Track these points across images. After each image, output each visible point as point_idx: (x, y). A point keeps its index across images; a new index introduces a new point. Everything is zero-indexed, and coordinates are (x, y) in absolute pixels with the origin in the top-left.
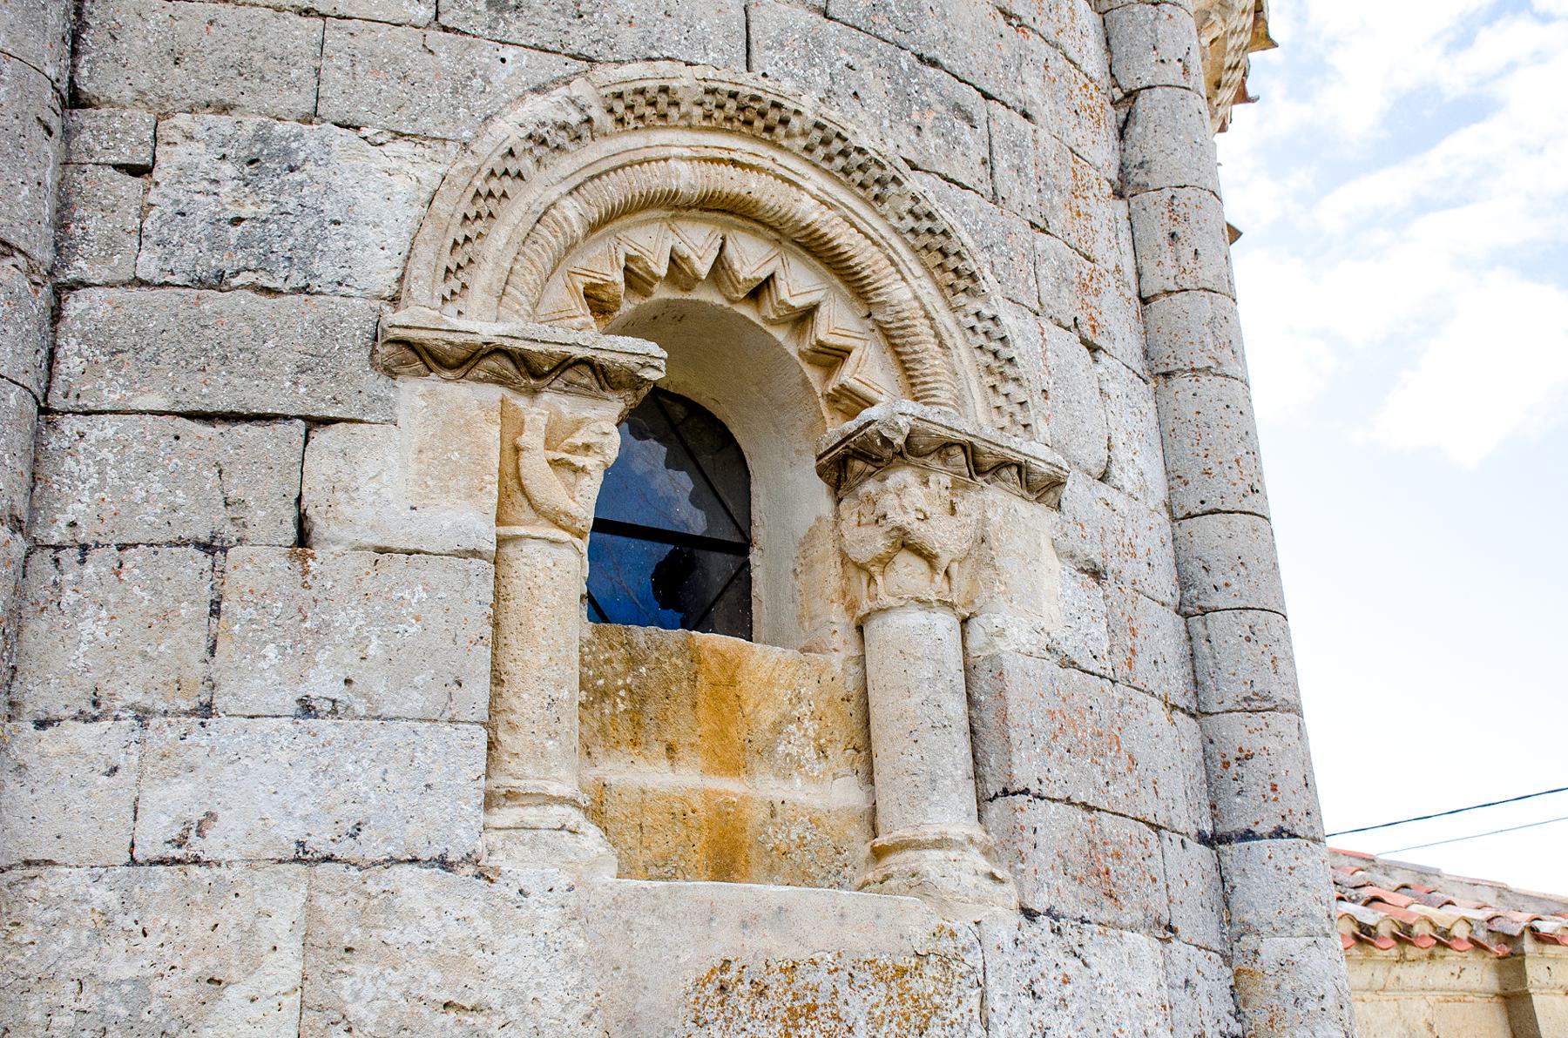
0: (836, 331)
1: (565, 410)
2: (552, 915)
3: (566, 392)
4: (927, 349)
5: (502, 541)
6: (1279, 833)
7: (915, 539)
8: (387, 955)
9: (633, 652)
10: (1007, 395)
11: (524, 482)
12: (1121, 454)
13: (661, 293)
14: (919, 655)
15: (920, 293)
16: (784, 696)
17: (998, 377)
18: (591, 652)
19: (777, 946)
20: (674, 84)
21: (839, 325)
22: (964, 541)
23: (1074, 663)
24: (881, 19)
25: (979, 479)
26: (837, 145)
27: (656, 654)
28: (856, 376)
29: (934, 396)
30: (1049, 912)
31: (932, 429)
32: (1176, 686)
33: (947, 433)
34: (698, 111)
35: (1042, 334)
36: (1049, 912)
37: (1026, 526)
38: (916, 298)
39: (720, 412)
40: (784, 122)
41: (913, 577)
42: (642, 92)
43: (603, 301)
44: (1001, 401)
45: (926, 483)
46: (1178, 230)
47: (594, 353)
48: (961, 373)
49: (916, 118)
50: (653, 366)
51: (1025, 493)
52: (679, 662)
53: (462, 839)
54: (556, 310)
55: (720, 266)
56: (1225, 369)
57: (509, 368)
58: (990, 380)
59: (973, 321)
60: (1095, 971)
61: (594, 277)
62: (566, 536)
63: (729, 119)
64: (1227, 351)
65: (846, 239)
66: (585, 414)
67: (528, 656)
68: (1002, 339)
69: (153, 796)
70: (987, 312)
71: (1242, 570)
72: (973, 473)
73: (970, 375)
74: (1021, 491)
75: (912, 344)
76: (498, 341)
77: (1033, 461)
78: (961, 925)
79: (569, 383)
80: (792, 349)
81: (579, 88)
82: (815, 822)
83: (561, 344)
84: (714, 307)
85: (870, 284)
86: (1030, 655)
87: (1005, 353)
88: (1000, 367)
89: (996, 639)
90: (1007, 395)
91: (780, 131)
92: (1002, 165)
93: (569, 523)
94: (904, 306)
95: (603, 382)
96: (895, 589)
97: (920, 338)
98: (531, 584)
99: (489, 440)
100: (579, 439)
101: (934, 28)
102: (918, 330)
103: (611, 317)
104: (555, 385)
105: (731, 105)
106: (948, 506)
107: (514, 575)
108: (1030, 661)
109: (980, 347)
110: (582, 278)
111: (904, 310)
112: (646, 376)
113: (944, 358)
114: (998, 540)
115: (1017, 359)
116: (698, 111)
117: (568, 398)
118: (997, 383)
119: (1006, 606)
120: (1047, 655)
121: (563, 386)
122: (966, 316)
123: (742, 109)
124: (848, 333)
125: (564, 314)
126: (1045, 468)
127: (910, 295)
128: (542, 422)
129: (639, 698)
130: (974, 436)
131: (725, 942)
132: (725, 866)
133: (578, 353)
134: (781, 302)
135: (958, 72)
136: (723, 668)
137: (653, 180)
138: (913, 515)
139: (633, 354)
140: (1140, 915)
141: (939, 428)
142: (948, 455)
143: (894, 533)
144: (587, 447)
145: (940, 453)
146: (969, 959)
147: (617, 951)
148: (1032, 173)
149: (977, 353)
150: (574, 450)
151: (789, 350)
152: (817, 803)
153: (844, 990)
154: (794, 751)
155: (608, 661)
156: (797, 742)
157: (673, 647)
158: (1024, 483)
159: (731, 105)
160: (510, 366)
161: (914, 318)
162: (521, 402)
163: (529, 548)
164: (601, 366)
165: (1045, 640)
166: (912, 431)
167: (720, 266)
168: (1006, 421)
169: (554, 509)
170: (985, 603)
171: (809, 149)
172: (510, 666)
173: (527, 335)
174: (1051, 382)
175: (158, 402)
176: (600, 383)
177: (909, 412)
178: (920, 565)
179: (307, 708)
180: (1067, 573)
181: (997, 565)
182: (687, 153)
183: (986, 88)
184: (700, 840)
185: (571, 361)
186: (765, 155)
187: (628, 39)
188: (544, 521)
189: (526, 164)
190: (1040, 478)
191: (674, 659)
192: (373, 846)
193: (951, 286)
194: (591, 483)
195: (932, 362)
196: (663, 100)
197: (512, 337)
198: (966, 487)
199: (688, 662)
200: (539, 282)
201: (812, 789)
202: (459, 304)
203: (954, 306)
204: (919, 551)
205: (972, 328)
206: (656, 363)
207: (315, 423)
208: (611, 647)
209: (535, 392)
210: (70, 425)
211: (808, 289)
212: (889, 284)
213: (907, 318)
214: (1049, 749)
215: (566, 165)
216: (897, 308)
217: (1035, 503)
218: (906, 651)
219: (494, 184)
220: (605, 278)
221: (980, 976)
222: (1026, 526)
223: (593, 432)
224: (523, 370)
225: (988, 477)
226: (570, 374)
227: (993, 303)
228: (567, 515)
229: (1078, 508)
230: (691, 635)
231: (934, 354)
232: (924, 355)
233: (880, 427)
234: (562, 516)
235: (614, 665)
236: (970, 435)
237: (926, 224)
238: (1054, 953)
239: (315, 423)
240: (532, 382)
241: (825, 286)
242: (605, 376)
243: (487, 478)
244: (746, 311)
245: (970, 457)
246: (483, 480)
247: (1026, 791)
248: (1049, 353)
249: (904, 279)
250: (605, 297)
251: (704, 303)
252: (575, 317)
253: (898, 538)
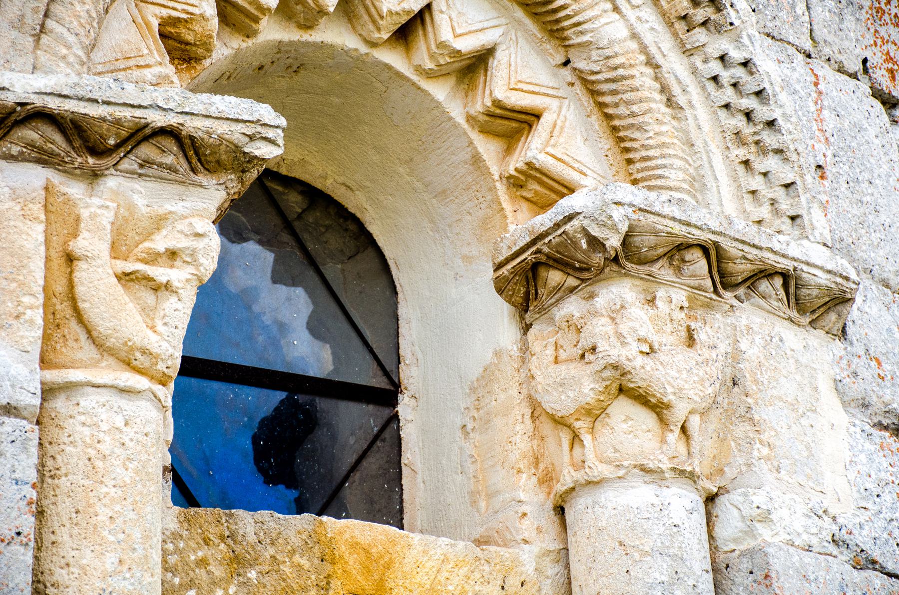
0: (520, 86)
1: (140, 201)
3: (140, 175)
4: (650, 111)
5: (48, 392)
7: (637, 381)
9: (238, 549)
10: (765, 174)
11: (82, 305)
14: (647, 548)
15: (640, 28)
17: (753, 148)
18: (177, 551)
21: (524, 77)
22: (707, 384)
23: (874, 562)
25: (728, 295)
27: (272, 551)
28: (549, 149)
29: (661, 177)
31: (662, 224)
33: (678, 229)
35: (816, 84)
37: (797, 361)
38: (634, 36)
39: (353, 202)
41: (636, 436)
43: (187, 43)
44: (757, 183)
45: (652, 301)
47: (180, 119)
48: (699, 143)
50: (265, 139)
51: (794, 314)
52: (304, 562)
54: (119, 55)
57: (57, 141)
58: (742, 153)
59: (715, 67)
61: (174, 9)
66: (168, 207)
67: (87, 558)
68: (759, 93)
70: (737, 55)
72: (719, 286)
73: (713, 147)
74: (788, 312)
75: (628, 103)
76: (39, 102)
77: (805, 268)
79: (146, 163)
80: (457, 111)
83: (133, 106)
84: (346, 52)
85: (568, 17)
86: (809, 549)
87: (763, 113)
88: (755, 133)
89: (758, 525)
90: (765, 174)
93: (147, 364)
94: (617, 49)
95: (194, 161)
96: (610, 454)
97: (639, 94)
98: (92, 452)
99: (29, 245)
100: (160, 243)
102: (637, 82)
103: (198, 67)
104: (125, 165)
106: (684, 334)
107: (66, 440)
108: (808, 558)
109: (727, 106)
110: (158, 10)
111: (616, 55)
112: (257, 153)
113: (675, 123)
114: (756, 382)
115: (781, 121)
117: (143, 183)
118: (752, 157)
119: (770, 477)
120: (832, 548)
121: (136, 166)
122: (706, 61)
124: (536, 89)
125: (132, 63)
126: (823, 279)
127: (624, 33)
128: (106, 218)
130: (720, 234)
133: (158, 119)
134: (442, 45)
136: (366, 570)
138: (634, 348)
139: (237, 121)
141: (670, 223)
142: (684, 261)
143: (608, 373)
144: (173, 254)
145: (671, 258)
149: (723, 113)
150: (153, 258)
151: (453, 114)
155: (202, 563)
157: (296, 541)
158: (792, 300)
160: (58, 138)
161: (631, 66)
162: (75, 189)
163: (89, 400)
164: (192, 138)
165: (829, 527)
166: (631, 228)
168: (765, 212)
169: (125, 344)
170: (741, 473)
172: (61, 575)
173: (81, 93)
174: (829, 154)
176: (190, 163)
177: (627, 200)
178: (645, 418)
180: (858, 430)
181: (757, 417)
185: (148, 131)
188: (111, 361)
190: (815, 292)
191: (297, 558)
193: (684, 18)
194: (179, 305)
195: (657, 128)
197: (60, 96)
198: (709, 306)
199: (316, 561)
200: (94, 15)
203: (688, 46)
204: (642, 399)
205: (715, 79)
206: (271, 134)
208: (207, 542)
209: (95, 175)
211: (479, 26)
212: (596, 17)
213: (622, 66)
216: (608, 52)
217: (809, 328)
218: (627, 542)
220: (190, 9)
222: (797, 361)
223: (181, 232)
224: (77, 144)
225: (741, 291)
226: (146, 150)
227: (745, 40)
228: (144, 352)
229: (872, 335)
230: (321, 523)
231: (660, 117)
232: (647, 118)
233: (586, 223)
234: (138, 355)
235: (211, 568)
236: (714, 233)
240: (91, 161)
241: (503, 21)
242: (197, 153)
243: (26, 300)
244: (393, 58)
245: (715, 265)
246: (19, 303)
248: (826, 113)
249: (616, 9)
250: (190, 38)
251: (331, 46)
252: (148, 66)
253: (614, 379)
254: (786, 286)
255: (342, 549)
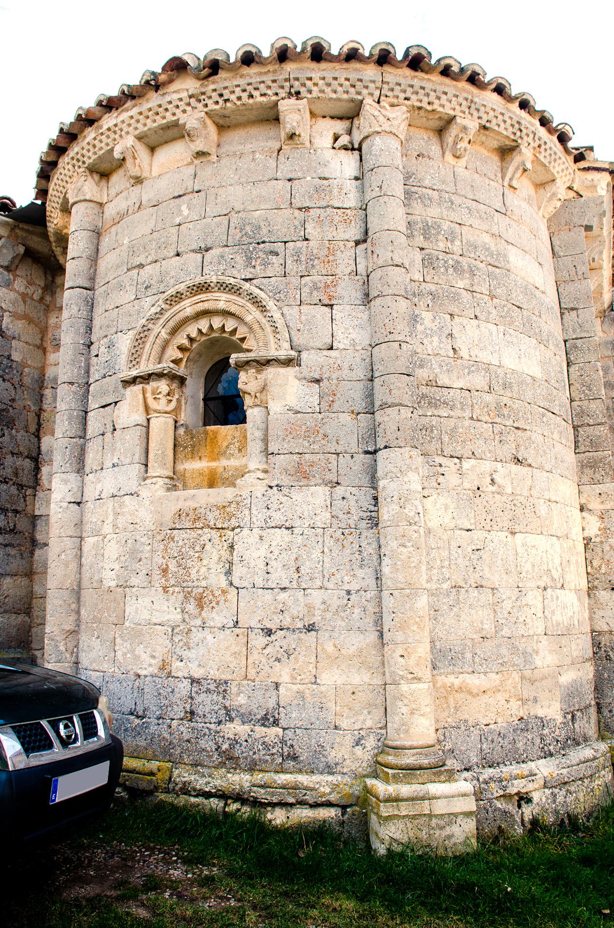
2: (148, 503)
5: (148, 420)
6: (386, 447)
8: (123, 514)
12: (339, 335)
13: (204, 338)
16: (229, 438)
19: (193, 504)
20: (178, 291)
24: (245, 238)
26: (224, 285)
30: (277, 486)
32: (360, 405)
33: (246, 359)
34: (188, 293)
36: (277, 486)
40: (209, 286)
42: (172, 296)
46: (373, 250)
49: (253, 264)
53: (134, 489)
55: (211, 327)
56: (383, 294)
57: (141, 380)
60: (294, 500)
62: (159, 415)
63: (197, 291)
64: (386, 287)
65: (233, 309)
69: (97, 487)
71: (383, 363)
78: (245, 493)
81: (160, 302)
82: (237, 469)
91: (210, 288)
92: (289, 262)
101: (264, 231)
105: (195, 288)
108: (280, 415)
116: (188, 293)
123: (198, 288)
126: (283, 357)
129: (193, 446)
131: (181, 505)
132: (211, 485)
133: (150, 372)
135: (273, 241)
137: (181, 315)
140: (321, 481)
144: (160, 392)
146: (245, 501)
147: (159, 509)
148: (303, 259)
150: (158, 394)
152: (237, 464)
153: (208, 513)
154: (232, 452)
156: (233, 449)
159: (195, 288)
167: (211, 327)
171: (219, 289)
175: (97, 406)
179: (114, 466)
182: (189, 305)
183: (285, 240)
184: (206, 479)
186: (209, 296)
187: (172, 281)
189: (150, 326)
192: (122, 493)
196: (178, 295)
198: (262, 370)
201: (236, 461)
202: (137, 367)
207: (116, 403)
210: (89, 414)
214: (284, 439)
215: (161, 321)
219: (142, 335)
221: (249, 505)
237: (251, 296)
238: (279, 496)
239: (116, 403)
247: (273, 453)
254: (276, 361)
255: (209, 432)
